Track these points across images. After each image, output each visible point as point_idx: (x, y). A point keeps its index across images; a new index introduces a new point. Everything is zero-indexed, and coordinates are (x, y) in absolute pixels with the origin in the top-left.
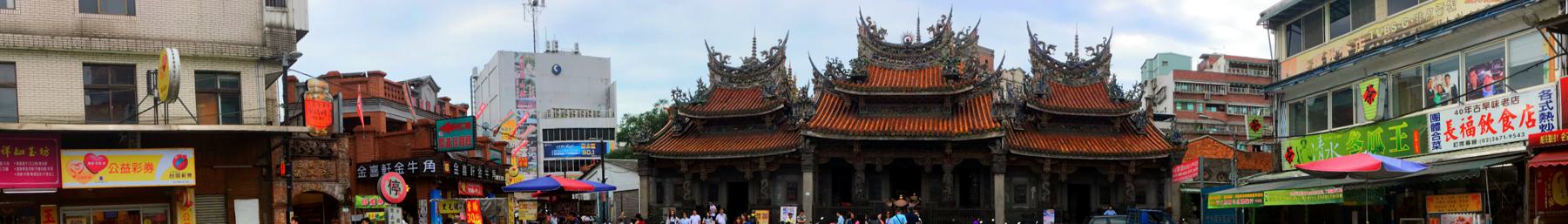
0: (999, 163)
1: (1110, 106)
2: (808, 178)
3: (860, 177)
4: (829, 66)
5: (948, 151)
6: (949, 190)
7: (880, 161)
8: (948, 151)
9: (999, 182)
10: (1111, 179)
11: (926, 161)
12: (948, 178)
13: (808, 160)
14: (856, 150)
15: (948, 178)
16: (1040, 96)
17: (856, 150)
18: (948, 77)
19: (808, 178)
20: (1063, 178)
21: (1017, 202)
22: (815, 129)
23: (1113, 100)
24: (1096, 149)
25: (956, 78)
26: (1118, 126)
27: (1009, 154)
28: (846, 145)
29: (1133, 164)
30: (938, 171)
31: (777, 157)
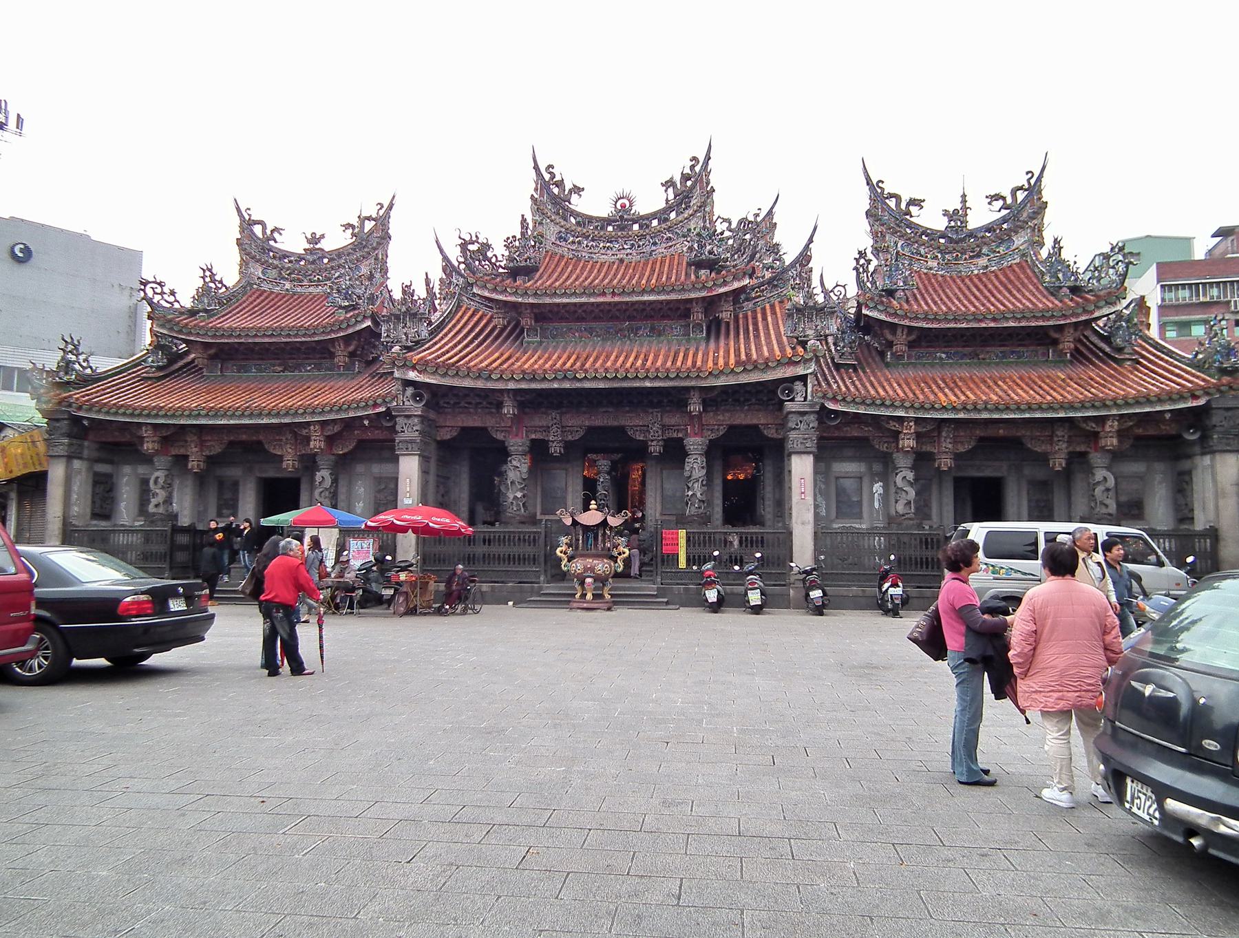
0: (801, 434)
1: (1050, 303)
2: (409, 468)
3: (517, 468)
4: (464, 246)
5: (695, 407)
6: (697, 490)
7: (558, 431)
8: (695, 407)
9: (801, 468)
10: (1059, 462)
11: (650, 429)
12: (695, 466)
13: (409, 431)
14: (509, 409)
15: (695, 466)
16: (890, 293)
17: (509, 409)
18: (699, 265)
19: (409, 468)
20: (945, 462)
21: (840, 514)
22: (422, 366)
23: (1054, 291)
24: (1022, 395)
25: (712, 265)
26: (1067, 344)
27: (824, 414)
28: (490, 400)
29: (1112, 426)
30: (675, 453)
31: (350, 424)
